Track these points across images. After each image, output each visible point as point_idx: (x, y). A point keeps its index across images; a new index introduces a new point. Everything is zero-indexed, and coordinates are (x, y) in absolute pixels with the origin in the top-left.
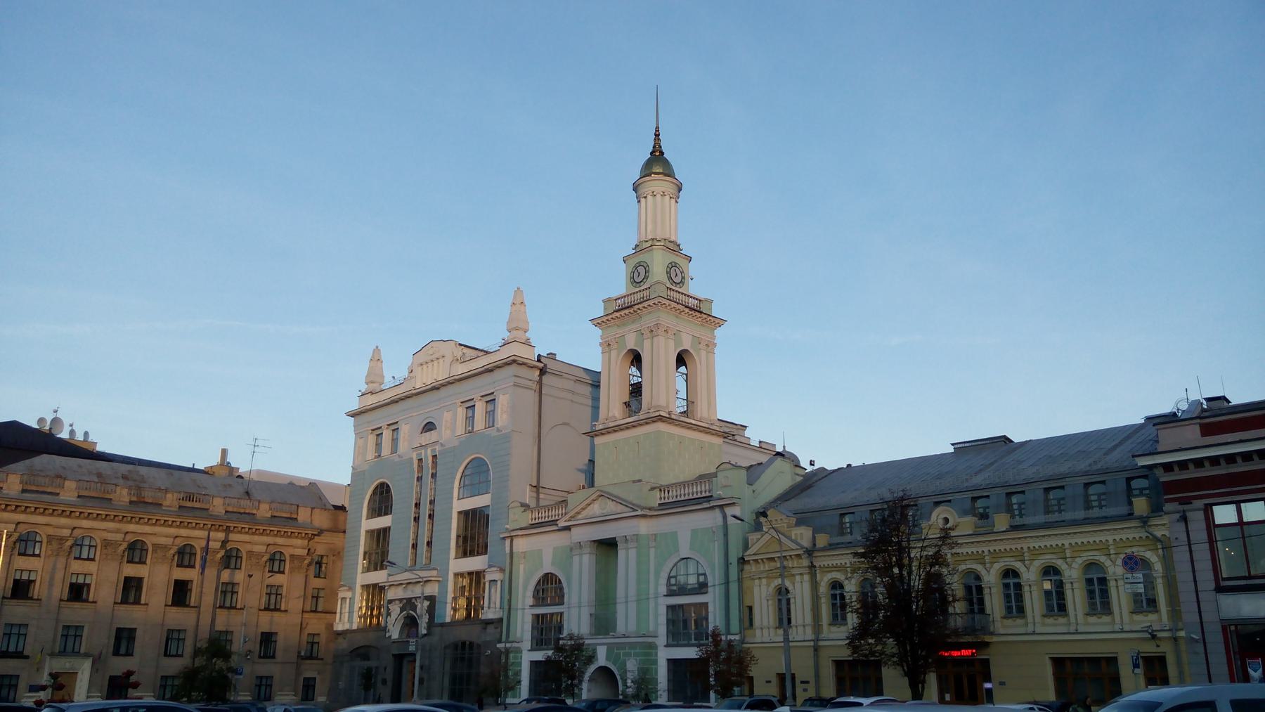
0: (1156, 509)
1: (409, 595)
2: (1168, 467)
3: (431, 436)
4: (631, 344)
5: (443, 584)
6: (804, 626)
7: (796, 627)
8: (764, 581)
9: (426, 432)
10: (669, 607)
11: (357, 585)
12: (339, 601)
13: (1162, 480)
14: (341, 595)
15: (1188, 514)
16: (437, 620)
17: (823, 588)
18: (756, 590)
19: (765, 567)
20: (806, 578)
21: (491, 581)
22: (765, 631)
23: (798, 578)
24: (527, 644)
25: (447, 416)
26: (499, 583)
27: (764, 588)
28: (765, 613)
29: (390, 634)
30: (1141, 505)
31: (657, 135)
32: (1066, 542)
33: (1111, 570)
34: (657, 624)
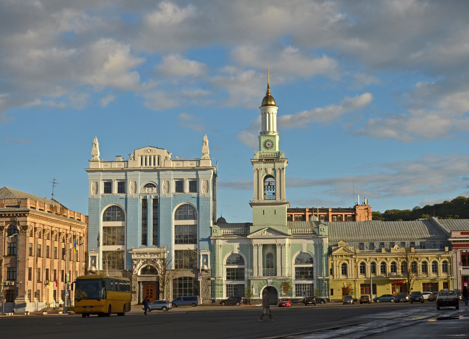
0: (450, 250)
1: (148, 257)
2: (454, 241)
5: (170, 255)
9: (148, 187)
10: (296, 268)
13: (452, 244)
14: (90, 255)
15: (457, 252)
16: (168, 268)
17: (359, 265)
18: (335, 264)
19: (338, 257)
20: (353, 261)
21: (203, 255)
24: (224, 279)
25: (163, 183)
26: (209, 256)
28: (338, 271)
29: (136, 273)
30: (447, 249)
31: (268, 87)
32: (429, 256)
33: (439, 263)
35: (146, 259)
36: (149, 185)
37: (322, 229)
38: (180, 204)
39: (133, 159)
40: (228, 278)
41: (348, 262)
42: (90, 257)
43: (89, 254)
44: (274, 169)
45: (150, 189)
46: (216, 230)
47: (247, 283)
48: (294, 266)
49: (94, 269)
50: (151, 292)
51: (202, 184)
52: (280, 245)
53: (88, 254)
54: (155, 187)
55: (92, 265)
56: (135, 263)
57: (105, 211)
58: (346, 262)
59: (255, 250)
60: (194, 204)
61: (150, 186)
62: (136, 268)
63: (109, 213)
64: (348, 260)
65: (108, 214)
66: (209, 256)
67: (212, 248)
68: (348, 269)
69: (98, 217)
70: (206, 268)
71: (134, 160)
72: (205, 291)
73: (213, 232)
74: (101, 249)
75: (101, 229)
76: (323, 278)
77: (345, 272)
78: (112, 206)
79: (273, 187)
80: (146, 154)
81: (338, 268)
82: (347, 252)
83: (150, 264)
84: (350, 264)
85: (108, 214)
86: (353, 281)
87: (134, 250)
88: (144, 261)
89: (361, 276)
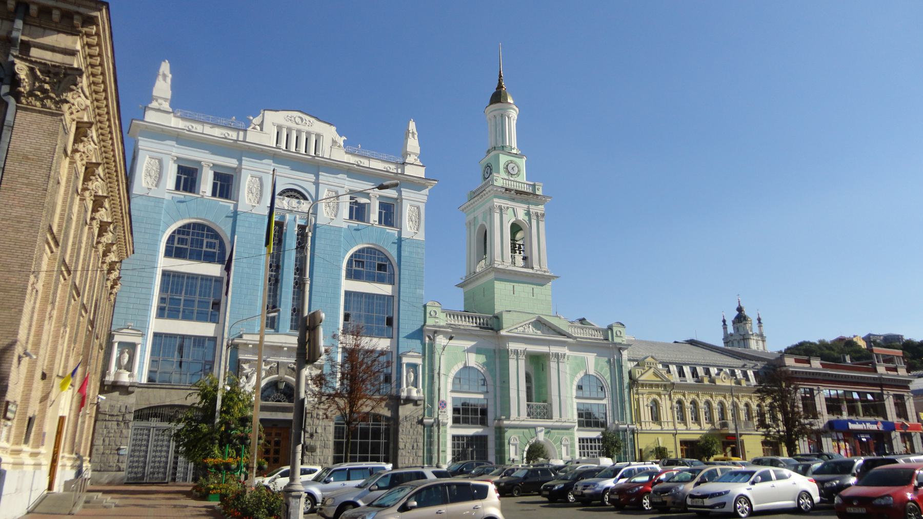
3: (305, 206)
4: (521, 216)
6: (668, 422)
7: (668, 422)
8: (645, 396)
9: (288, 196)
11: (150, 330)
12: (116, 345)
14: (117, 338)
20: (667, 396)
22: (647, 424)
23: (663, 396)
27: (645, 399)
28: (646, 414)
34: (573, 414)
35: (275, 362)
36: (293, 193)
37: (618, 333)
38: (355, 249)
39: (258, 128)
40: (456, 421)
41: (661, 398)
42: (116, 345)
43: (116, 336)
44: (528, 213)
45: (294, 202)
46: (435, 312)
47: (493, 433)
48: (575, 401)
49: (125, 378)
50: (277, 448)
51: (407, 210)
52: (557, 356)
53: (114, 335)
54: (305, 198)
55: (119, 366)
56: (244, 369)
57: (174, 232)
58: (658, 398)
59: (512, 363)
60: (389, 250)
61: (294, 196)
62: (248, 382)
63: (183, 239)
64: (659, 395)
65: (181, 241)
66: (421, 366)
67: (429, 353)
68: (661, 411)
69: (156, 244)
70: (414, 394)
71: (262, 130)
72: (411, 448)
73: (428, 315)
74: (150, 327)
75: (157, 275)
76: (626, 426)
77: (656, 418)
78: (195, 224)
79: (520, 248)
80: (293, 125)
81: (646, 408)
82: (659, 379)
83: (286, 376)
84: (664, 401)
85: (181, 241)
86: (672, 435)
87: (245, 337)
88: (271, 367)
89: (681, 427)
